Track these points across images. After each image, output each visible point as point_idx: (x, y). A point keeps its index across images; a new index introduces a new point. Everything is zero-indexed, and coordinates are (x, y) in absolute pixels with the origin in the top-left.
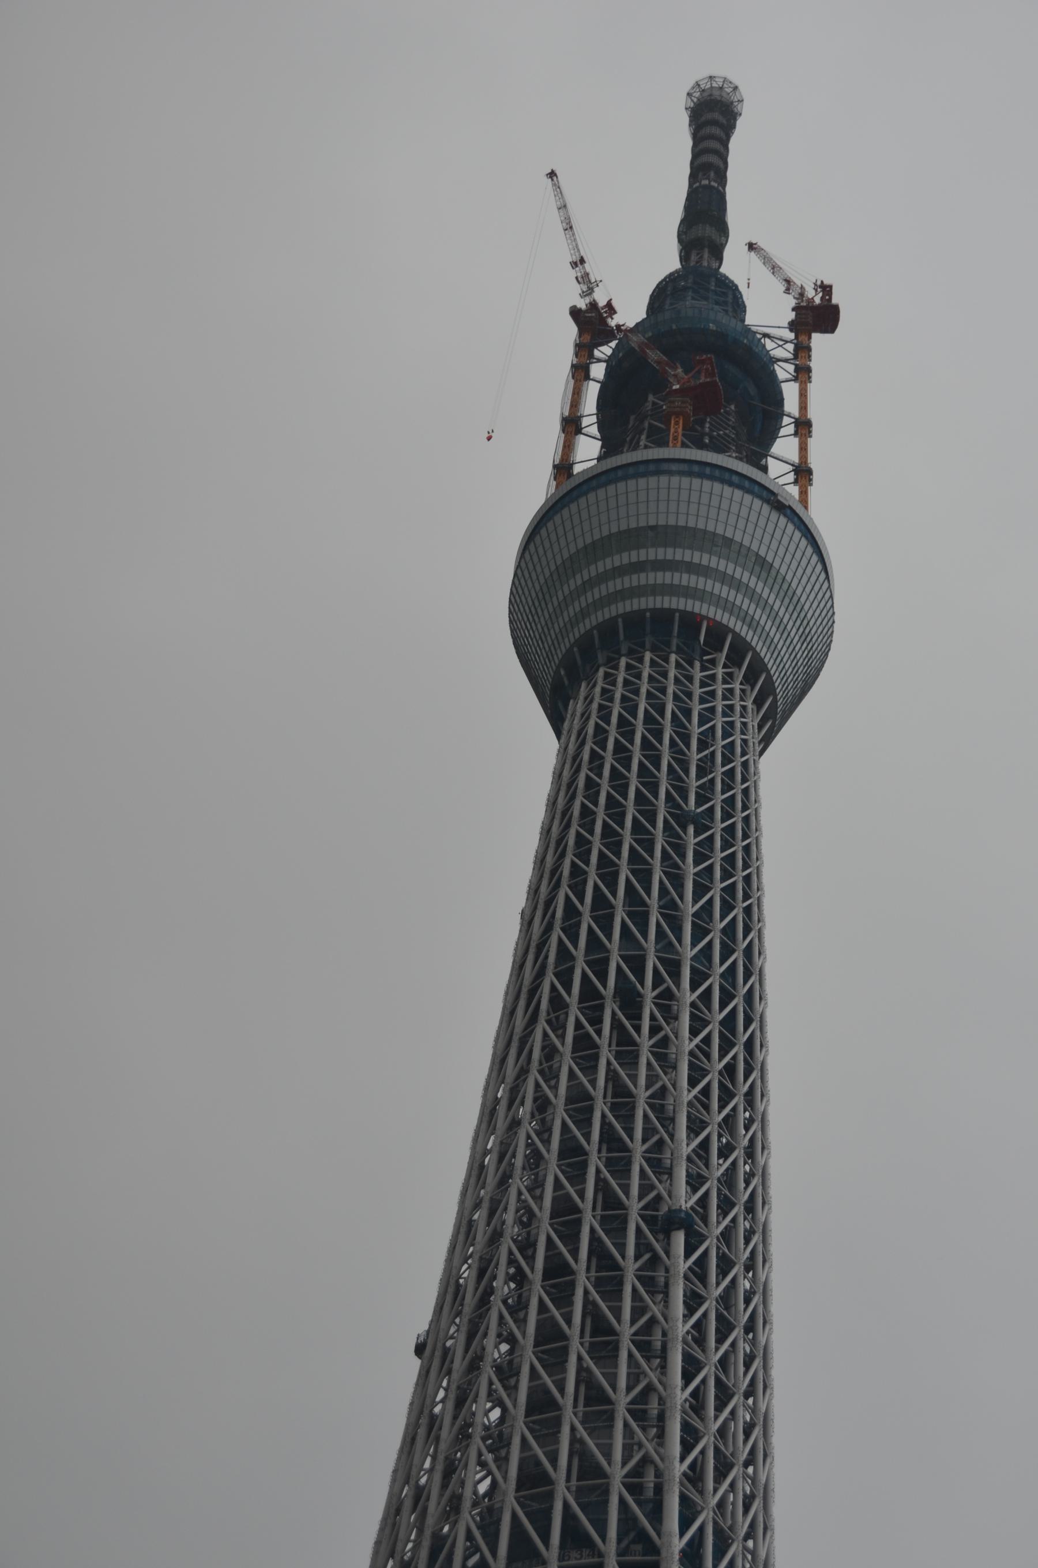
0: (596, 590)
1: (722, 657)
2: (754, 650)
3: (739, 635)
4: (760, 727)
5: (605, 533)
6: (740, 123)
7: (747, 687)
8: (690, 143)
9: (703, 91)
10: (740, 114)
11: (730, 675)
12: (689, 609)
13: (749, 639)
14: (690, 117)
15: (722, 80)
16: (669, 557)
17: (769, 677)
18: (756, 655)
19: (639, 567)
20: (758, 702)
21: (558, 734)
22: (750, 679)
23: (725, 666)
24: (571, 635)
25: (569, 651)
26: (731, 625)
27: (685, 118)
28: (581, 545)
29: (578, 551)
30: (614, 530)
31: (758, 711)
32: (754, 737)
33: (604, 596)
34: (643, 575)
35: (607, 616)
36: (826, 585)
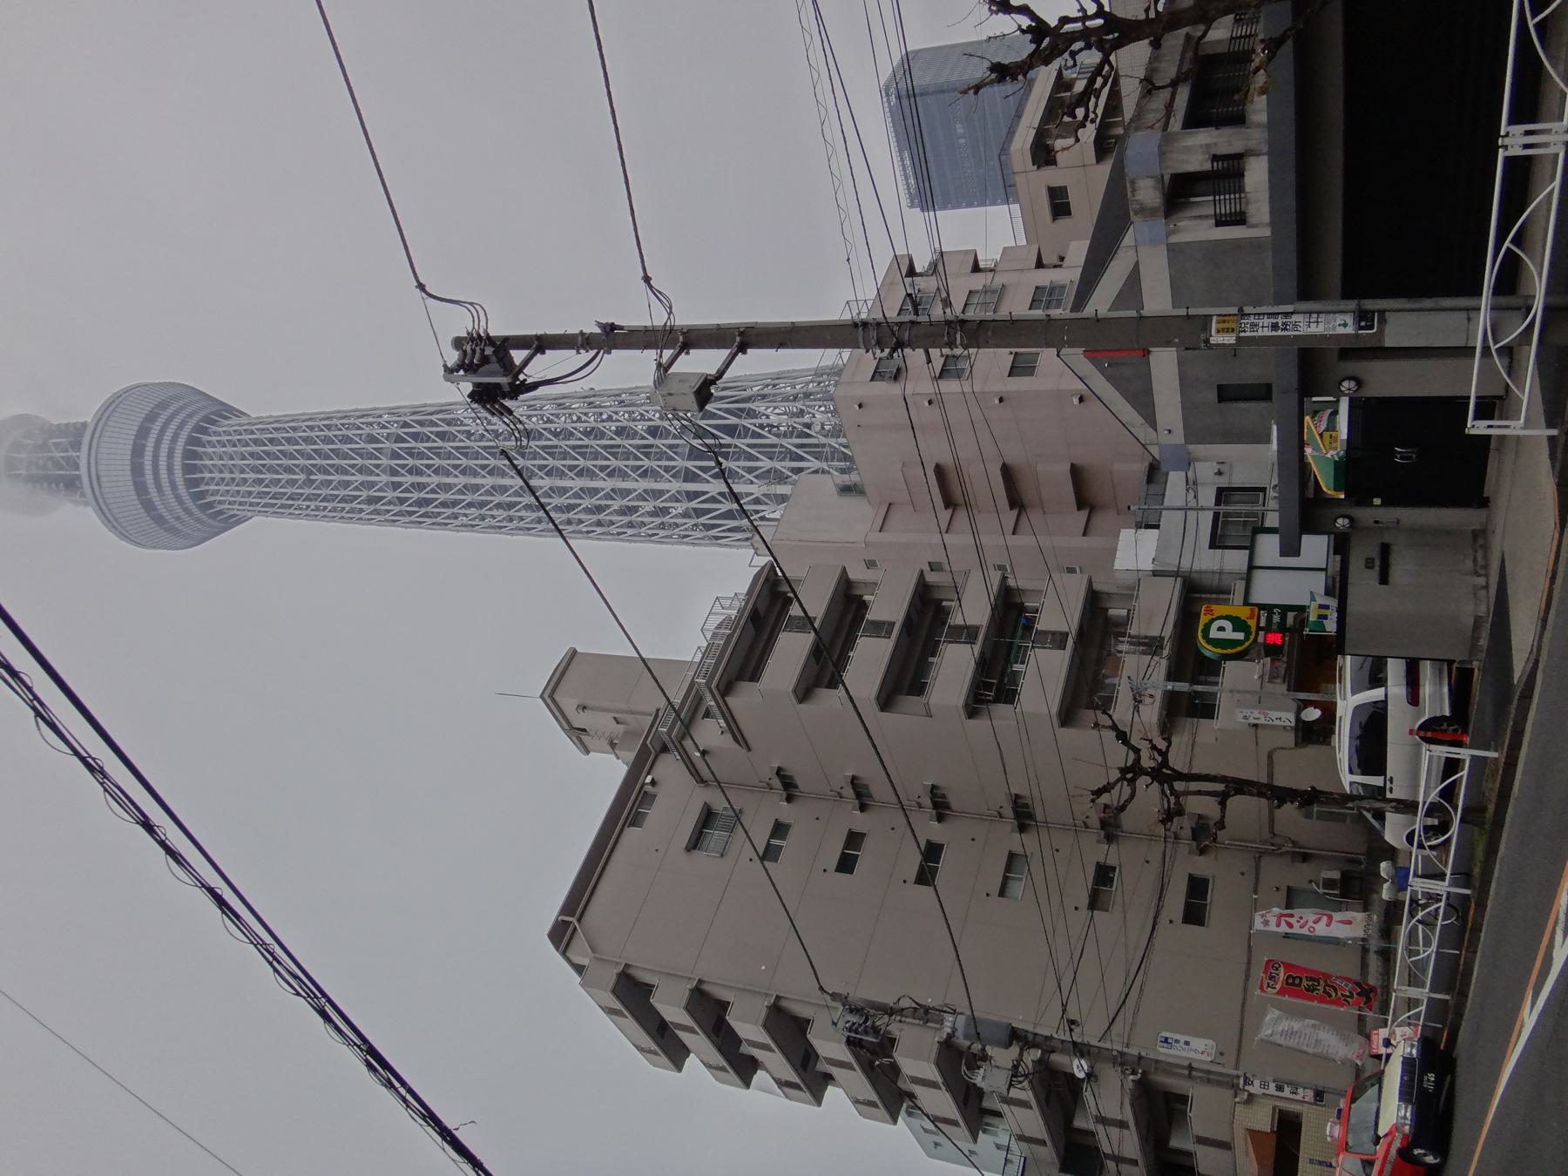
1: (205, 438)
3: (192, 429)
5: (137, 502)
7: (218, 423)
11: (214, 432)
12: (180, 455)
18: (202, 420)
20: (226, 418)
22: (213, 422)
23: (210, 436)
29: (149, 516)
30: (136, 497)
32: (244, 420)
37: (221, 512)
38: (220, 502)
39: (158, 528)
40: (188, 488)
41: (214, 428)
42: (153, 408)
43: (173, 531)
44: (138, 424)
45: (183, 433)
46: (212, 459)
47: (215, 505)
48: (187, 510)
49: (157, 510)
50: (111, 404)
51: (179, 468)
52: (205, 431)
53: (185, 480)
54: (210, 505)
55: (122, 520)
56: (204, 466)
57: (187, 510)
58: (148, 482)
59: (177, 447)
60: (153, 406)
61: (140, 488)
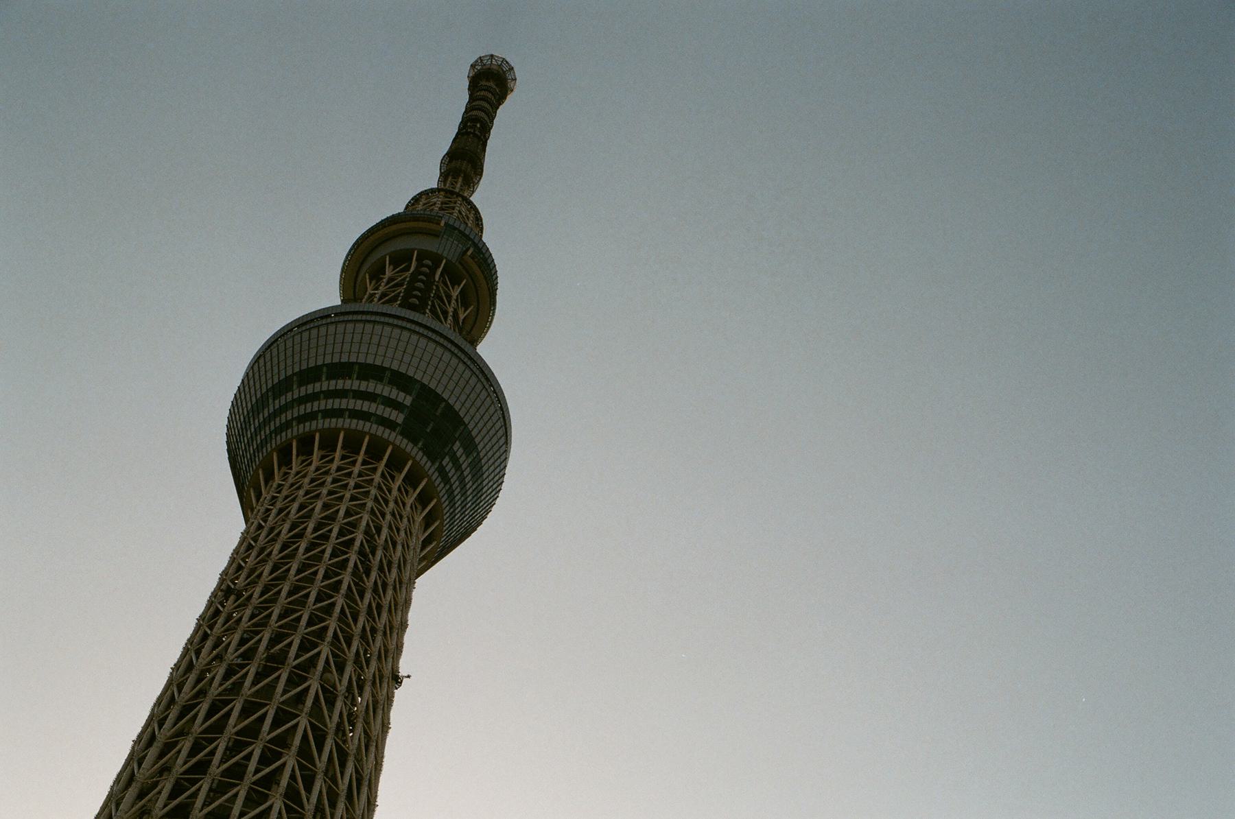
0: (302, 407)
2: (430, 479)
4: (425, 544)
5: (320, 363)
6: (510, 98)
7: (419, 507)
8: (465, 97)
9: (485, 65)
10: (512, 91)
13: (426, 469)
14: (470, 82)
15: (501, 60)
16: (371, 390)
17: (439, 504)
19: (341, 394)
21: (246, 523)
22: (423, 499)
24: (273, 442)
25: (270, 455)
26: (413, 454)
27: (466, 83)
28: (297, 370)
29: (294, 374)
30: (328, 360)
31: (425, 530)
33: (276, 384)
34: (344, 401)
35: (307, 429)
36: (503, 440)
37: (269, 477)
38: (286, 474)
39: (270, 385)
40: (322, 432)
41: (410, 501)
42: (466, 426)
43: (262, 403)
44: (445, 396)
45: (415, 450)
46: (360, 475)
47: (284, 469)
48: (287, 425)
49: (300, 386)
50: (488, 379)
51: (360, 428)
52: (412, 480)
53: (336, 432)
54: (285, 460)
55: (297, 338)
56: (354, 463)
57: (287, 425)
58: (348, 382)
59: (393, 434)
60: (470, 427)
61: (340, 370)
